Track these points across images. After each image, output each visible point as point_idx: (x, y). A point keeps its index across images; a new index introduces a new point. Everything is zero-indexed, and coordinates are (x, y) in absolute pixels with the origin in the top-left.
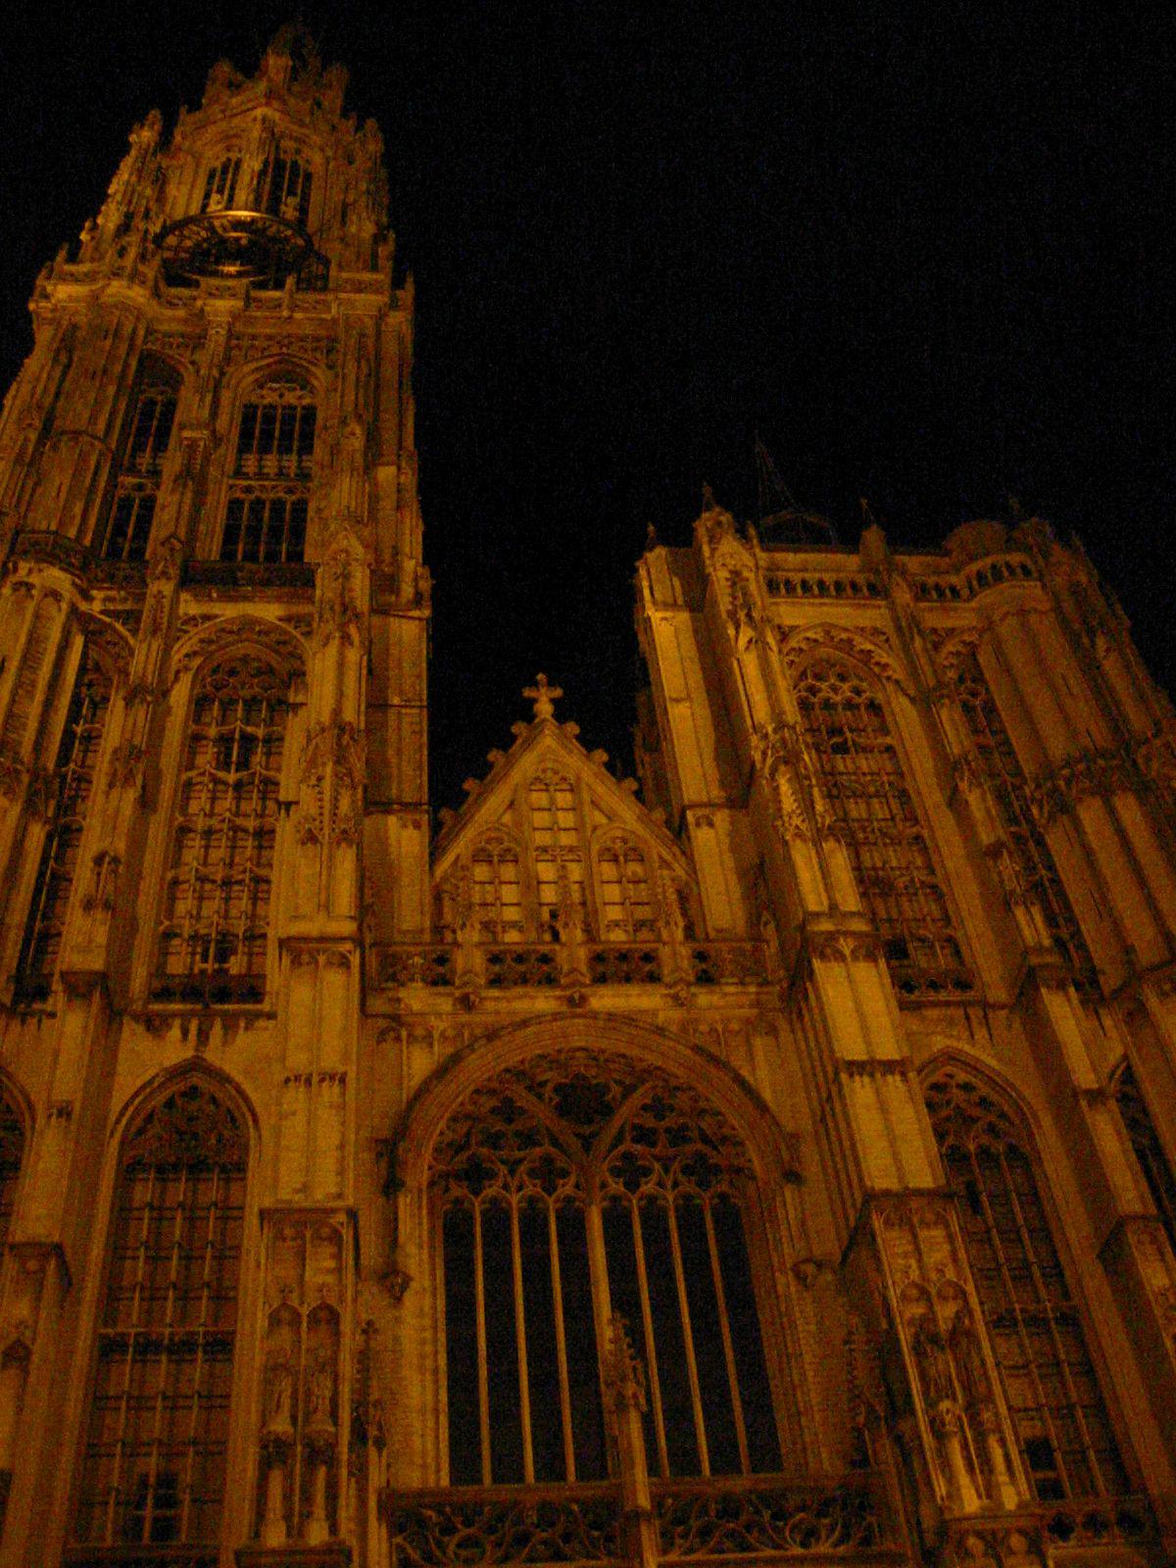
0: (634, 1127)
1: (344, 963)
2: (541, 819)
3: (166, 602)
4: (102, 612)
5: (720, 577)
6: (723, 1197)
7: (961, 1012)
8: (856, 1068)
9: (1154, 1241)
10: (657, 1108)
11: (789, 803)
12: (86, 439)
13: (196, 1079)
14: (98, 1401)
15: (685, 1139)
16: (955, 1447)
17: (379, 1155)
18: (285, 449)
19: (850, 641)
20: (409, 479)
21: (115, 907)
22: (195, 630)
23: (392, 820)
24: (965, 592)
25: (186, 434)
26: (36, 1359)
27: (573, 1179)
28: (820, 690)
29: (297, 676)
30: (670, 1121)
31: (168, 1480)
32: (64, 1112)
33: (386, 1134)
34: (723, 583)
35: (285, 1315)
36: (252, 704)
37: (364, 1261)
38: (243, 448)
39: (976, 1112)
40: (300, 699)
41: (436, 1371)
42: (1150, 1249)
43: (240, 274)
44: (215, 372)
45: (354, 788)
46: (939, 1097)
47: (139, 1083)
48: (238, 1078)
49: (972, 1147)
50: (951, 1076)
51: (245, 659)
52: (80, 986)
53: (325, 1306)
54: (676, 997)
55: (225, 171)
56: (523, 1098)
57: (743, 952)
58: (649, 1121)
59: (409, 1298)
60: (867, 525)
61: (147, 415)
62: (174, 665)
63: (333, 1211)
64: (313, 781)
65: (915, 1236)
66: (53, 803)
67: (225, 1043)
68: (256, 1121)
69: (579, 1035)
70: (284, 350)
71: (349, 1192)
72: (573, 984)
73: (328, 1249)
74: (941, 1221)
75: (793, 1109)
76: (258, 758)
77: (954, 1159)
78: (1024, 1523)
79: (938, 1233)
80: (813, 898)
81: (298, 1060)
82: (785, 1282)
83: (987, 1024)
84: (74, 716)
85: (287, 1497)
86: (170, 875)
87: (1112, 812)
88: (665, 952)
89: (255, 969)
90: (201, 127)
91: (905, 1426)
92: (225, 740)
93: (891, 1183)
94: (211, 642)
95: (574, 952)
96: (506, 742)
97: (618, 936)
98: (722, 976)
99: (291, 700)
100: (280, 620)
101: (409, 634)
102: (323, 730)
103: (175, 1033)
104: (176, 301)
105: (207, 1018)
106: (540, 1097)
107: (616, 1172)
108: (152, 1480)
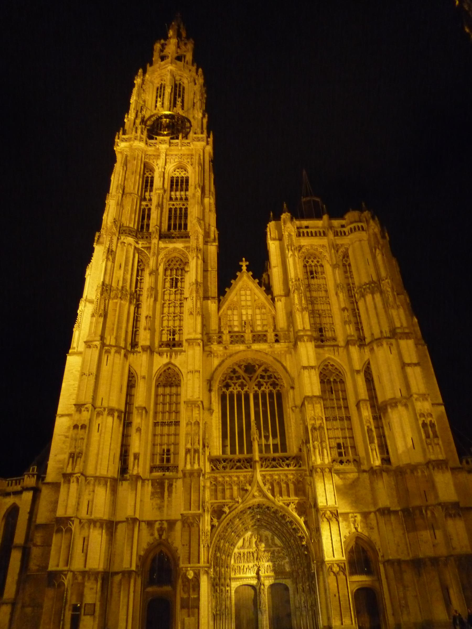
0: (261, 375)
1: (199, 345)
2: (243, 298)
3: (156, 245)
4: (142, 247)
5: (286, 234)
6: (278, 391)
7: (333, 348)
8: (305, 368)
9: (366, 405)
10: (266, 370)
11: (296, 301)
12: (133, 195)
13: (170, 366)
14: (154, 435)
15: (271, 378)
16: (317, 451)
17: (208, 383)
18: (182, 190)
19: (317, 248)
20: (212, 201)
21: (152, 330)
23: (209, 302)
24: (347, 234)
25: (157, 192)
26: (142, 430)
29: (187, 263)
30: (268, 374)
31: (168, 451)
32: (144, 378)
34: (287, 236)
35: (189, 423)
36: (177, 269)
37: (205, 406)
38: (171, 190)
39: (334, 371)
40: (188, 270)
41: (219, 428)
42: (365, 407)
43: (167, 135)
44: (163, 170)
45: (200, 299)
47: (158, 368)
50: (329, 363)
51: (175, 257)
52: (145, 349)
54: (270, 346)
55: (161, 88)
56: (237, 369)
57: (285, 334)
58: (264, 374)
59: (214, 414)
60: (324, 214)
61: (147, 182)
62: (159, 262)
63: (198, 401)
65: (314, 406)
66: (135, 300)
67: (175, 358)
68: (182, 375)
69: (250, 356)
71: (201, 397)
72: (248, 344)
73: (197, 409)
74: (320, 403)
75: (293, 372)
76: (179, 284)
77: (323, 391)
78: (328, 466)
80: (300, 327)
81: (190, 368)
82: (289, 411)
84: (137, 276)
85: (191, 459)
86: (162, 316)
87: (373, 298)
88: (269, 335)
89: (181, 340)
90: (153, 72)
91: (308, 445)
92: (172, 279)
93: (310, 394)
94: (167, 254)
95: (248, 336)
96: (235, 277)
97: (259, 328)
101: (213, 249)
102: (193, 284)
103: (165, 355)
104: (151, 145)
106: (240, 368)
107: (256, 385)
108: (165, 451)
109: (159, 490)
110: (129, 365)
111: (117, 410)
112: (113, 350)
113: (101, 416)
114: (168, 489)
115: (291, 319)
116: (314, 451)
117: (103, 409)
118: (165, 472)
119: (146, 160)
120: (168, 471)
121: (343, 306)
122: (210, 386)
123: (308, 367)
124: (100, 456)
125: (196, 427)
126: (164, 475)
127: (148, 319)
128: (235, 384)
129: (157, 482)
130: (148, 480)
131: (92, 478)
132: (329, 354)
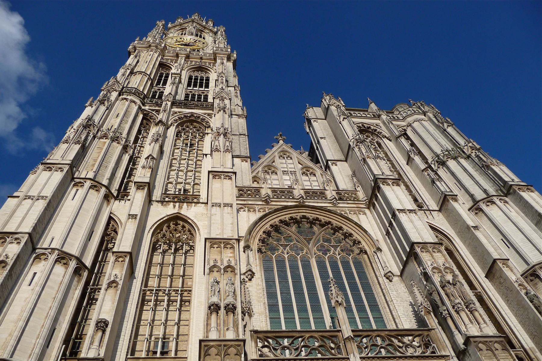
48: (192, 219)
67: (187, 210)
68: (198, 230)
70: (200, 64)
99: (206, 132)
110: (111, 213)
123: (404, 210)
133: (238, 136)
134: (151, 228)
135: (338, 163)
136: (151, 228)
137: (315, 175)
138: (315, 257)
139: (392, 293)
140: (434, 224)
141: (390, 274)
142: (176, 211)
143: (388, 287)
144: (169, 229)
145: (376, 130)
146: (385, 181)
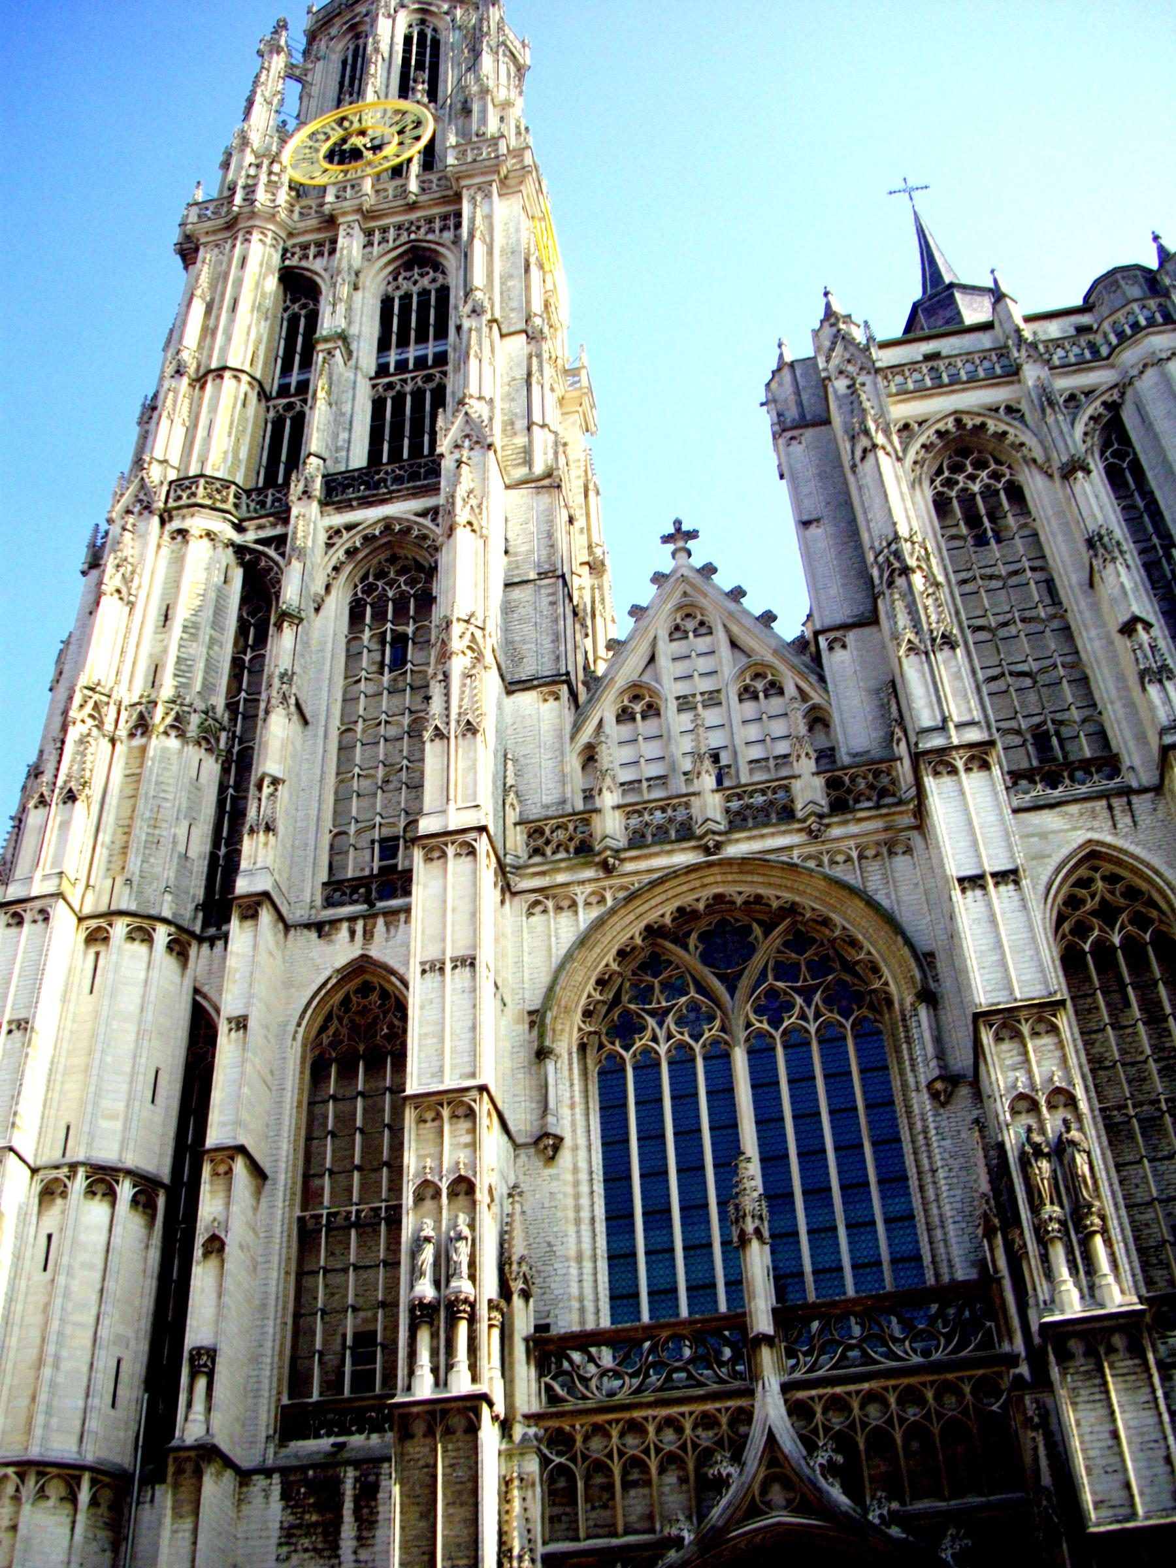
7: (1104, 803)
16: (1058, 1253)
17: (532, 1024)
18: (422, 339)
22: (342, 541)
24: (1104, 351)
27: (717, 1023)
28: (957, 483)
32: (241, 1023)
33: (536, 1005)
35: (430, 1192)
46: (1082, 893)
47: (315, 987)
49: (1116, 940)
53: (461, 1179)
59: (565, 1156)
63: (467, 1089)
64: (441, 677)
65: (1025, 1046)
67: (387, 940)
70: (413, 236)
79: (1047, 1041)
81: (432, 953)
83: (1131, 810)
85: (434, 1353)
88: (797, 785)
98: (857, 801)
100: (418, 515)
105: (370, 917)
107: (759, 1011)
108: (349, 1342)
109: (314, 1518)
110: (196, 991)
111: (129, 1172)
112: (120, 928)
113: (59, 1201)
114: (357, 1512)
115: (894, 708)
116: (1045, 1258)
117: (66, 1170)
118: (351, 1433)
119: (287, 263)
120: (360, 1432)
121: (1124, 617)
122: (541, 1036)
123: (981, 877)
124: (47, 1371)
125: (462, 1200)
126: (341, 1446)
127: (266, 791)
128: (660, 1016)
129: (307, 1482)
130: (268, 1472)
131: (10, 1471)
132: (1092, 829)
133: (531, 586)
134: (299, 1025)
135: (851, 637)
136: (299, 1025)
137: (781, 692)
138: (747, 1040)
139: (943, 1143)
140: (1132, 848)
141: (939, 1086)
142: (354, 951)
143: (932, 1126)
144: (347, 1010)
145: (1005, 433)
146: (941, 761)
